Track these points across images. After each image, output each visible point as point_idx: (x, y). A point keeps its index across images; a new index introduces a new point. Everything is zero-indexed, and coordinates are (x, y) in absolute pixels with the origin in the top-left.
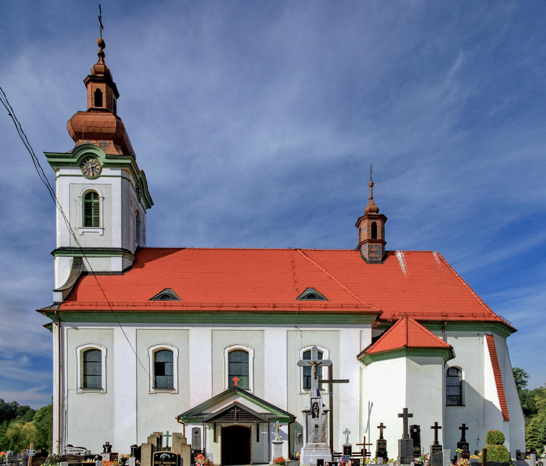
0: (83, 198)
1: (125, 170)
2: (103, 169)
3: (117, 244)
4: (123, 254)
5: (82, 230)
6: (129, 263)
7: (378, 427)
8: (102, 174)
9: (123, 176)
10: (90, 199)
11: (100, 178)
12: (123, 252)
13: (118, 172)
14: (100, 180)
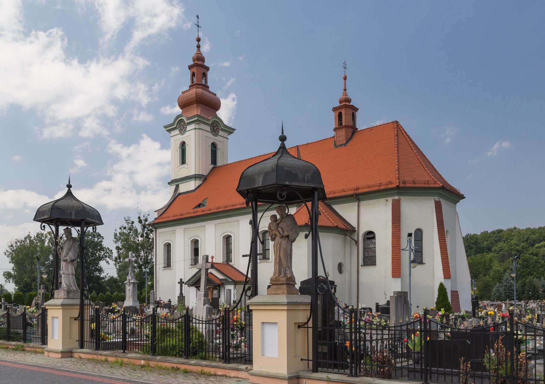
0: (179, 147)
3: (193, 173)
4: (195, 178)
5: (179, 168)
6: (201, 182)
8: (187, 130)
9: (196, 128)
11: (186, 133)
12: (195, 177)
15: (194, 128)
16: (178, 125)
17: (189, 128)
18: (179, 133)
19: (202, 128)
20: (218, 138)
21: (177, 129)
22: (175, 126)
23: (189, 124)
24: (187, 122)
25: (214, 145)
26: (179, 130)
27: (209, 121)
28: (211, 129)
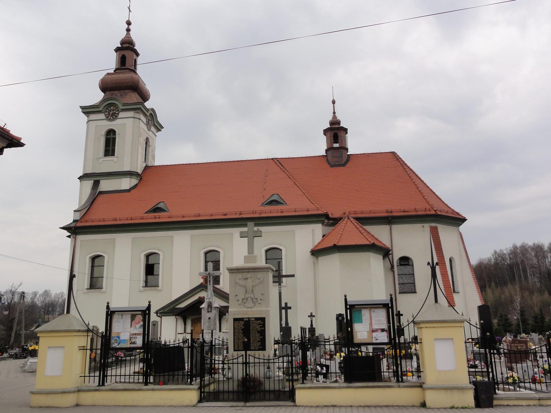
1: (136, 112)
2: (120, 113)
7: (309, 316)
8: (118, 117)
13: (131, 114)
14: (118, 122)
15: (132, 116)
16: (105, 108)
17: (122, 115)
18: (104, 118)
19: (143, 120)
20: (150, 133)
21: (103, 113)
22: (100, 109)
23: (123, 110)
24: (121, 107)
25: (147, 141)
26: (106, 115)
27: (148, 112)
28: (147, 122)
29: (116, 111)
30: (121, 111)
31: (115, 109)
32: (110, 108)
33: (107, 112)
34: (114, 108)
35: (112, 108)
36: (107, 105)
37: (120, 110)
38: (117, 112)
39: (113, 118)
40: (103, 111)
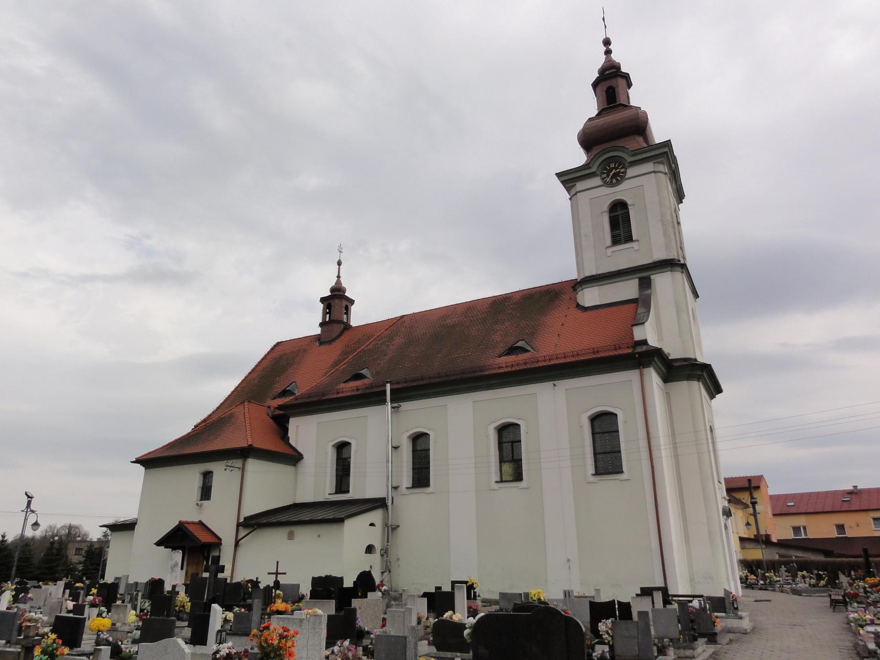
2: (627, 170)
8: (627, 177)
9: (656, 170)
10: (616, 211)
11: (626, 181)
13: (649, 167)
14: (625, 185)
15: (653, 170)
17: (631, 172)
18: (601, 183)
21: (597, 175)
22: (594, 169)
24: (630, 159)
29: (621, 169)
30: (629, 167)
31: (619, 166)
32: (609, 166)
33: (604, 173)
34: (615, 165)
35: (612, 165)
36: (604, 161)
37: (627, 165)
38: (622, 170)
39: (617, 180)
40: (598, 173)
